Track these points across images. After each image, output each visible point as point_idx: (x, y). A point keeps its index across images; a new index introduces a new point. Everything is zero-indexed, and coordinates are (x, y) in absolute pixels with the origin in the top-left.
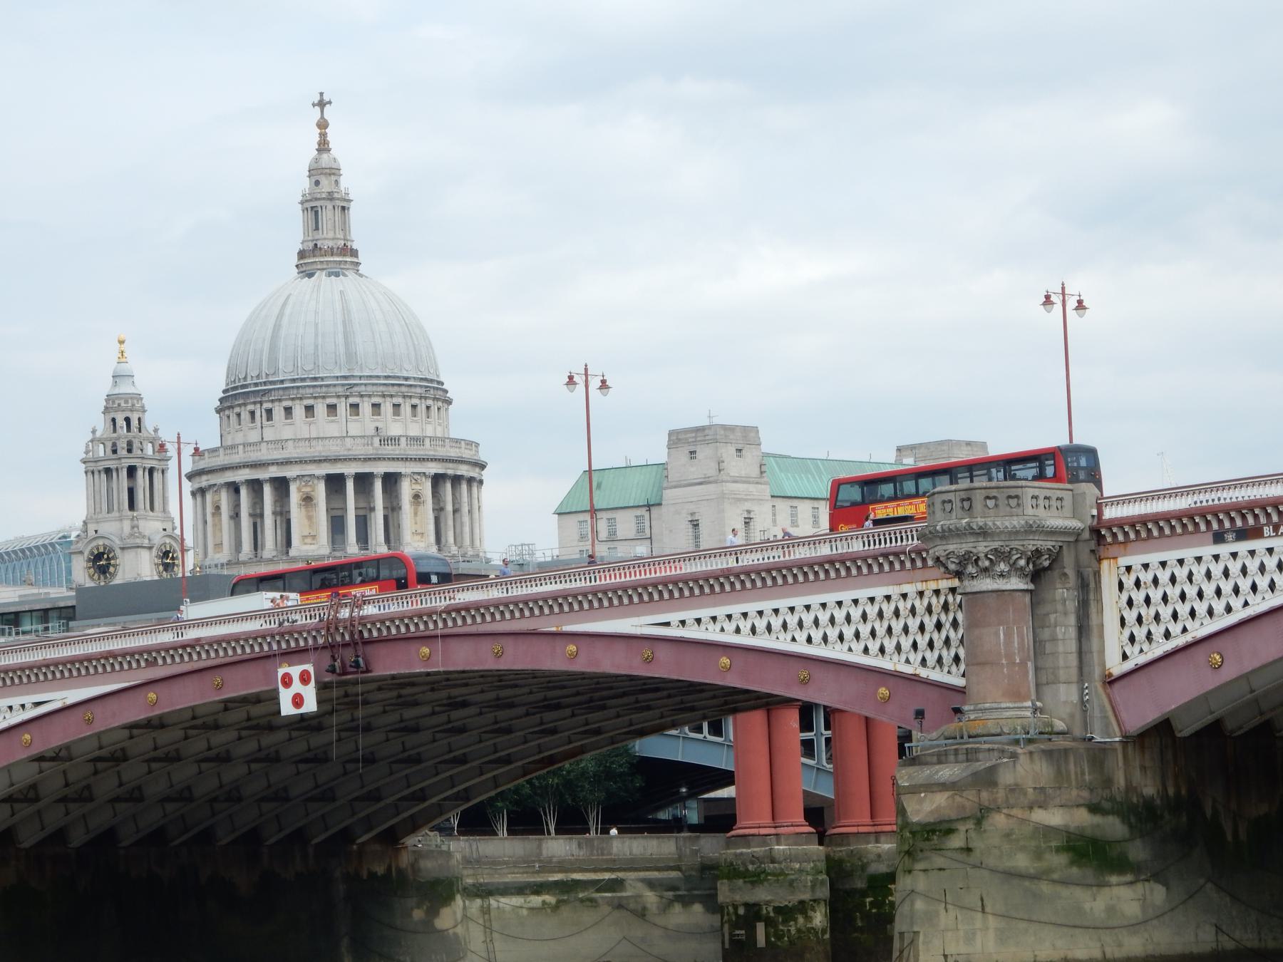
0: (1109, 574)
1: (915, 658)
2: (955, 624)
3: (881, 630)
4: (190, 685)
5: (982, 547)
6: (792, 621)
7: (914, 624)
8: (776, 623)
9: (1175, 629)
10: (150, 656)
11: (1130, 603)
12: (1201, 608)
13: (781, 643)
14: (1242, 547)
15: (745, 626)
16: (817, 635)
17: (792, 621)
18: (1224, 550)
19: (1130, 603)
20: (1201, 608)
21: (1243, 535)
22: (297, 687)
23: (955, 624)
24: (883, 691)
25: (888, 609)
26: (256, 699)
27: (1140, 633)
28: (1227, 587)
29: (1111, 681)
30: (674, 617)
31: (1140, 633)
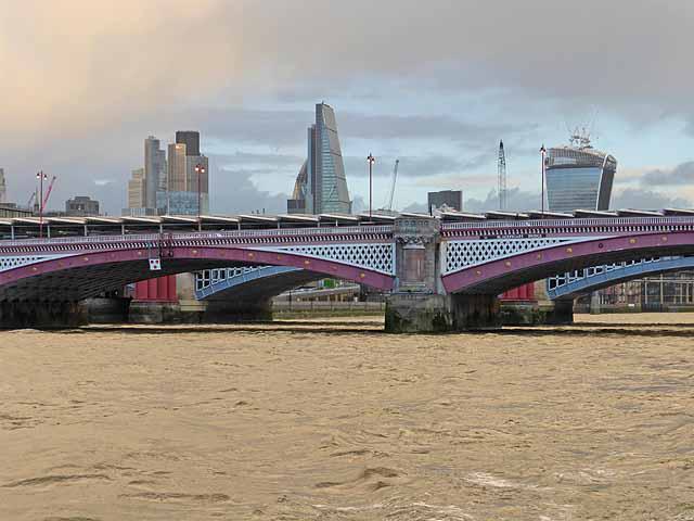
0: (443, 246)
1: (355, 261)
2: (389, 257)
3: (363, 256)
4: (103, 256)
5: (418, 236)
6: (332, 252)
7: (375, 256)
8: (326, 252)
9: (465, 263)
10: (86, 246)
11: (450, 254)
12: (474, 258)
13: (328, 258)
14: (490, 241)
15: (320, 252)
16: (340, 257)
17: (332, 252)
18: (483, 241)
19: (450, 254)
20: (474, 258)
21: (489, 238)
22: (155, 264)
23: (389, 257)
24: (363, 275)
25: (366, 251)
26: (138, 262)
27: (453, 264)
28: (483, 252)
29: (442, 277)
30: (289, 247)
31: (453, 264)
